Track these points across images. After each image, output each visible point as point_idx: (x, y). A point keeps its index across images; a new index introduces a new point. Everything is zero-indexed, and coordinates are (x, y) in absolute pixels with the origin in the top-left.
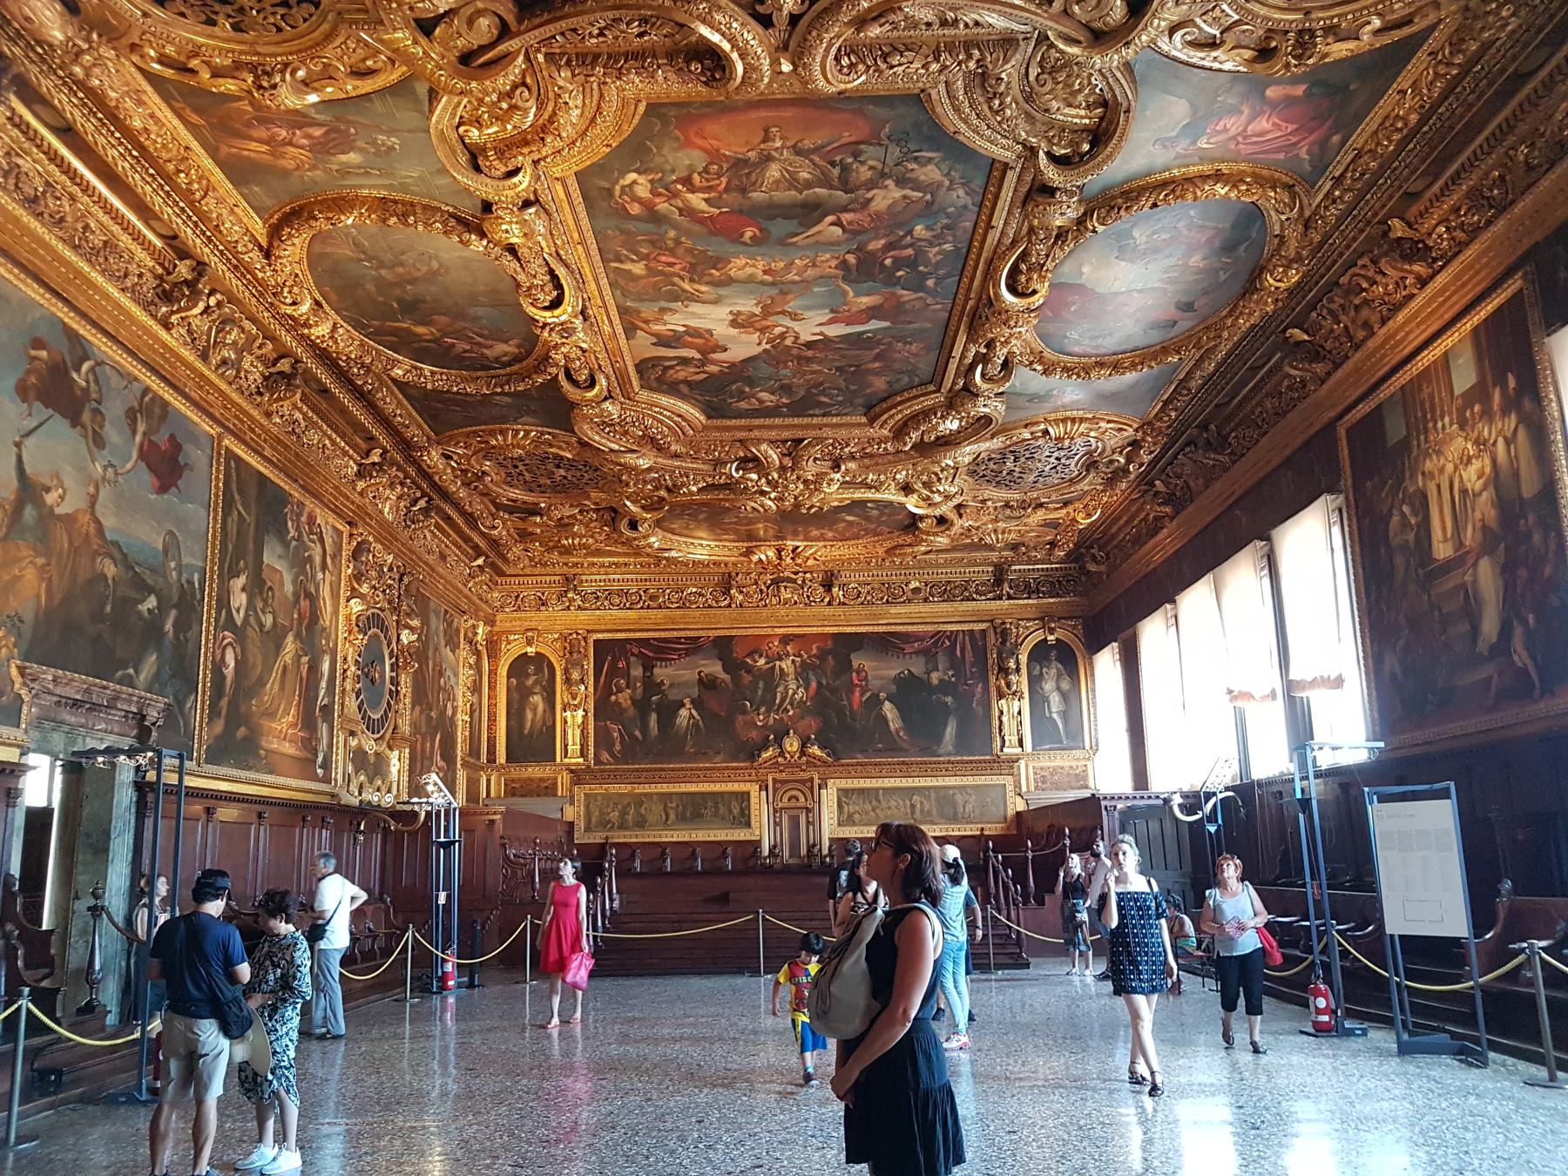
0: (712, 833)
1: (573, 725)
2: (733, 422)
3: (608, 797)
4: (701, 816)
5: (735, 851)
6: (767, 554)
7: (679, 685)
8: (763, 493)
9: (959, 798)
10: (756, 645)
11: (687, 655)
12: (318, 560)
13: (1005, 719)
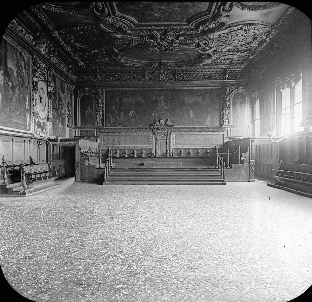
2: (146, 24)
8: (155, 46)
12: (23, 66)
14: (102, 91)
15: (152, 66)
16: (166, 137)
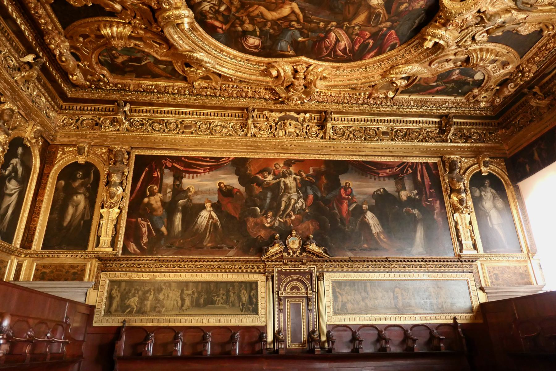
3: (130, 283)
4: (213, 302)
5: (242, 336)
6: (284, 67)
7: (202, 192)
10: (265, 166)
13: (460, 227)
15: (274, 73)
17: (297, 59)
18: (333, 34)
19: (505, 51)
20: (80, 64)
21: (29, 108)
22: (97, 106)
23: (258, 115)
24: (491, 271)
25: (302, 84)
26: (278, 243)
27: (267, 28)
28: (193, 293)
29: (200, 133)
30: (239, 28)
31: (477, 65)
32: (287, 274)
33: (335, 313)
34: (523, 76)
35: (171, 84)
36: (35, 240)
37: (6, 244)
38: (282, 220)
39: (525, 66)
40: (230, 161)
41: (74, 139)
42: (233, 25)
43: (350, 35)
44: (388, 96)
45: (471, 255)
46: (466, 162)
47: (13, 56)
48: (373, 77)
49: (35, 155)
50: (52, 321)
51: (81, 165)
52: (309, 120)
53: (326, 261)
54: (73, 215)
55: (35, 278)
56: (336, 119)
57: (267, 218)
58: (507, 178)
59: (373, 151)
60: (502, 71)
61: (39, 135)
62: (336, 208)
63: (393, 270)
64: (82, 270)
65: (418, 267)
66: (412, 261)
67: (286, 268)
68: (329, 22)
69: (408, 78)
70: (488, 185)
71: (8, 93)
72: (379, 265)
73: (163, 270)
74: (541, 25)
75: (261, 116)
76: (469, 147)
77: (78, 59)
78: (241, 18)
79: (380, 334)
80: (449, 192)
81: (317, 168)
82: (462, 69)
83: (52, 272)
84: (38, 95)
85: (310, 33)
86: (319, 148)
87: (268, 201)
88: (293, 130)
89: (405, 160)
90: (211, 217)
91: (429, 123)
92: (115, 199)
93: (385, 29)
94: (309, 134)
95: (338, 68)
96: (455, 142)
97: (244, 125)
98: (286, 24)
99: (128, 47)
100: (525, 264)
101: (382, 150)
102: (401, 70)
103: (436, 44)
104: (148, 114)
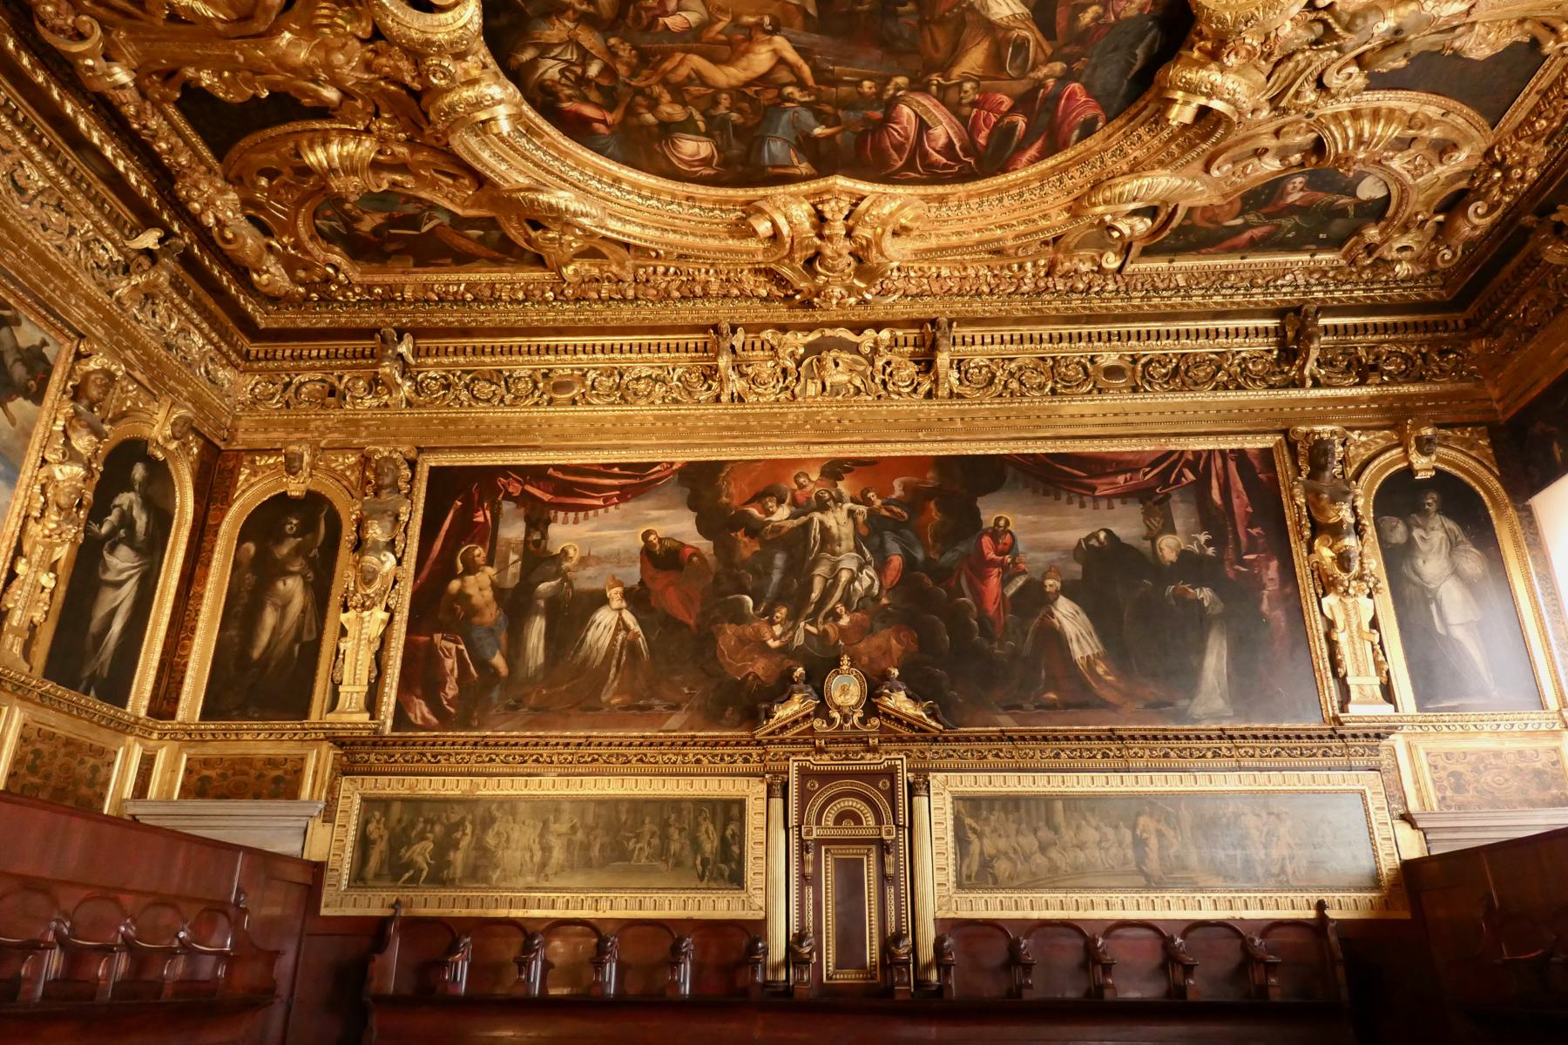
0: (649, 898)
1: (363, 638)
3: (414, 804)
4: (624, 855)
6: (789, 210)
7: (599, 560)
9: (1250, 821)
10: (770, 482)
11: (623, 498)
13: (1341, 637)
14: (407, 473)
15: (763, 227)
16: (879, 821)
17: (821, 184)
18: (905, 110)
19: (1433, 111)
20: (274, 243)
21: (159, 362)
22: (332, 345)
23: (749, 342)
24: (1441, 763)
25: (845, 252)
26: (801, 691)
27: (722, 110)
28: (573, 829)
29: (595, 401)
30: (649, 118)
31: (1347, 159)
32: (826, 777)
33: (960, 885)
34: (1506, 178)
35: (506, 276)
36: (183, 697)
37: (105, 708)
38: (813, 630)
39: (1508, 148)
40: (674, 472)
41: (278, 435)
42: (631, 111)
43: (955, 109)
44: (1105, 265)
45: (1375, 719)
46: (1364, 444)
47: (108, 237)
48: (1045, 217)
49: (180, 482)
50: (191, 900)
51: (296, 500)
52: (890, 348)
53: (935, 740)
54: (275, 631)
55: (186, 792)
56: (968, 340)
57: (772, 623)
58: (1496, 485)
59: (1079, 426)
60: (1439, 169)
61: (183, 429)
62: (967, 592)
63: (1133, 763)
64: (296, 772)
65: (1209, 754)
66: (1187, 738)
67: (823, 762)
68: (888, 80)
69: (1151, 212)
70: (1433, 508)
71: (99, 332)
72: (1090, 750)
73: (497, 767)
74: (1528, 26)
75: (758, 344)
76: (1373, 399)
77: (266, 231)
78: (647, 91)
79: (1089, 945)
80: (1307, 533)
81: (915, 479)
82: (1311, 173)
83: (223, 776)
84: (181, 330)
85: (840, 113)
86: (919, 425)
87: (776, 576)
88: (844, 378)
89: (1174, 445)
90: (622, 625)
91: (1247, 335)
92: (377, 585)
93: (1051, 82)
94: (890, 387)
95: (942, 199)
96: (1330, 386)
97: (710, 374)
98: (771, 94)
99: (375, 190)
100: (1555, 744)
101: (1102, 420)
102: (1117, 190)
103: (1204, 112)
104: (462, 359)
